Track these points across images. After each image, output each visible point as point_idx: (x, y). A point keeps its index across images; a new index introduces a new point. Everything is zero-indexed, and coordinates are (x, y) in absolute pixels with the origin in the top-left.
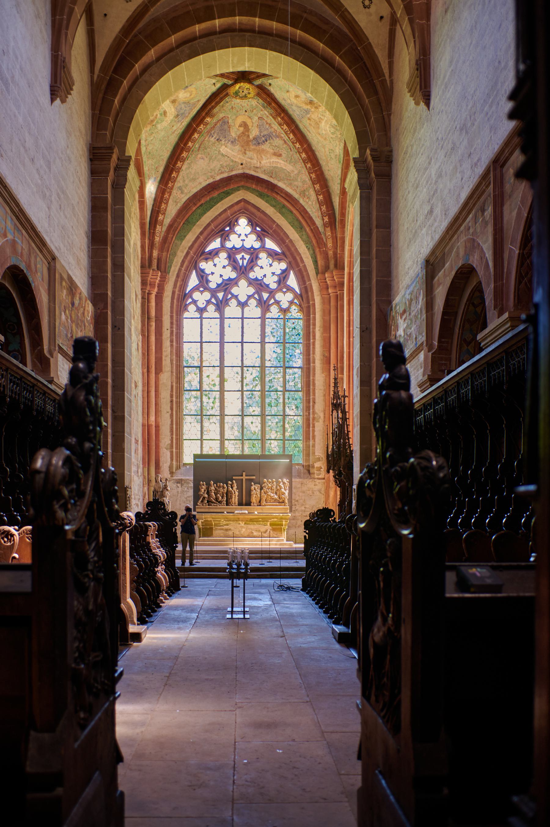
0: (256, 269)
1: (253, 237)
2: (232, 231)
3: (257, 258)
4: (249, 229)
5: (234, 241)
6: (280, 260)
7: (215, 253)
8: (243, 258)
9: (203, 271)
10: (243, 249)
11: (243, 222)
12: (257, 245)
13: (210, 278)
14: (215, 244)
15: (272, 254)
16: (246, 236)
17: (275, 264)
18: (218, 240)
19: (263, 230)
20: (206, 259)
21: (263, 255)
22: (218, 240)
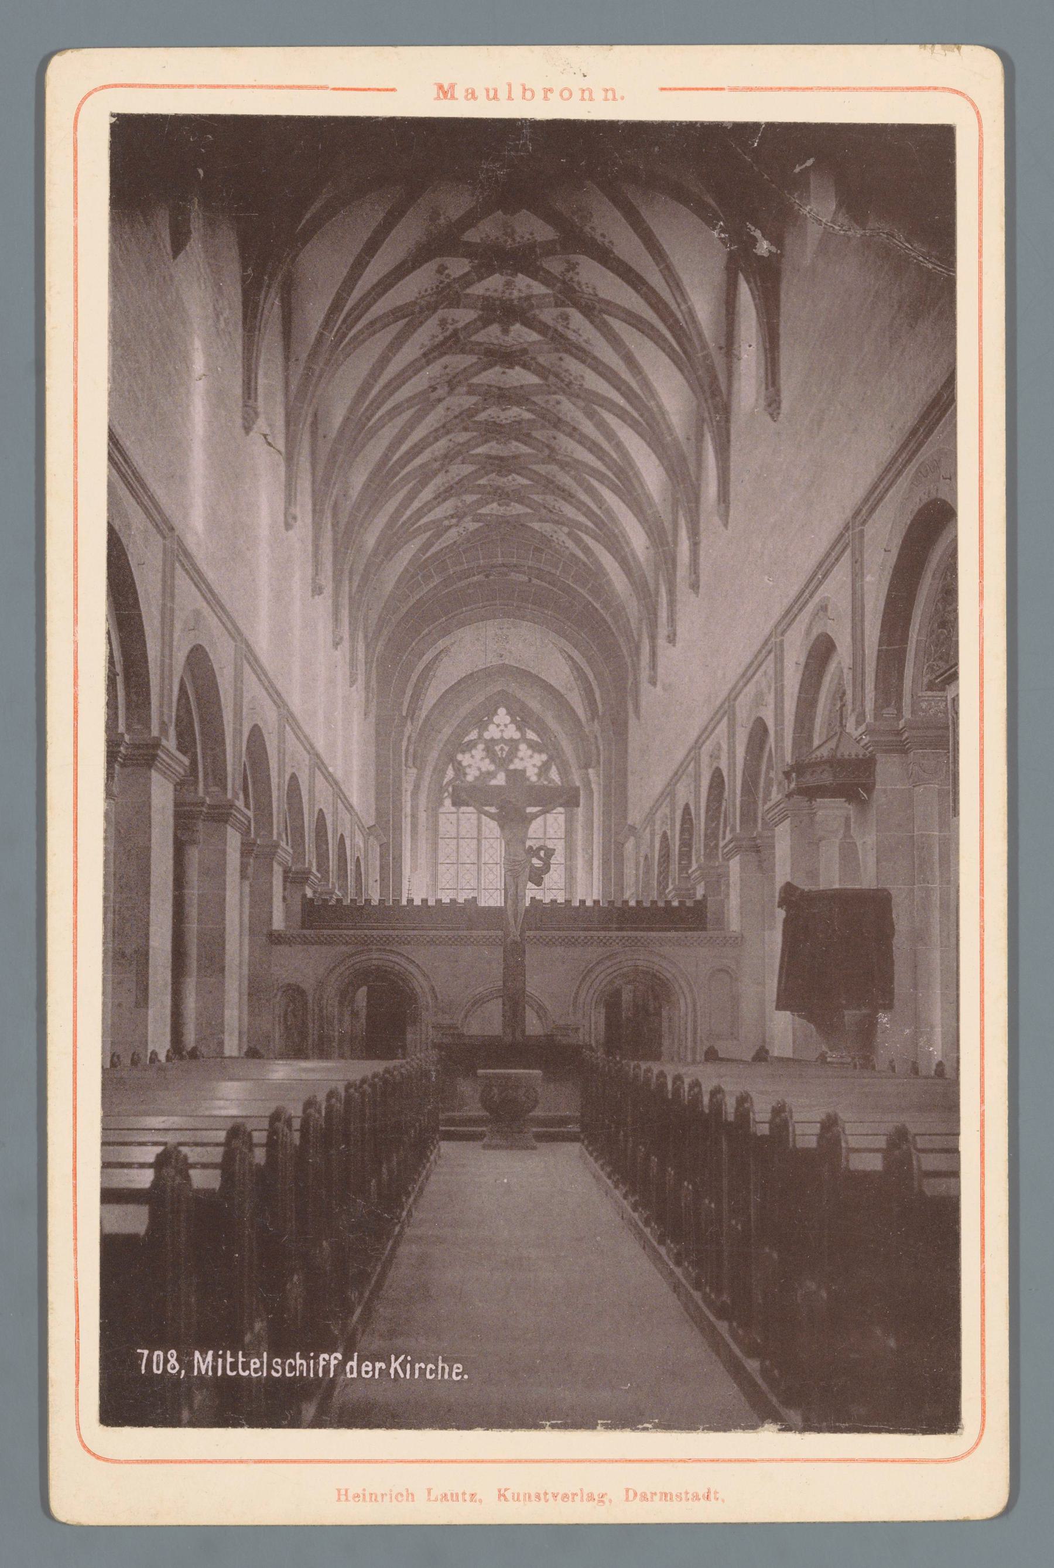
0: (516, 761)
1: (513, 727)
2: (491, 721)
3: (517, 749)
4: (508, 719)
5: (492, 732)
6: (540, 752)
7: (471, 746)
8: (502, 749)
9: (460, 763)
10: (502, 740)
11: (502, 711)
12: (517, 735)
13: (468, 770)
14: (473, 735)
15: (532, 746)
16: (506, 726)
17: (536, 756)
18: (476, 732)
19: (523, 720)
20: (463, 752)
21: (523, 747)
22: (476, 732)
